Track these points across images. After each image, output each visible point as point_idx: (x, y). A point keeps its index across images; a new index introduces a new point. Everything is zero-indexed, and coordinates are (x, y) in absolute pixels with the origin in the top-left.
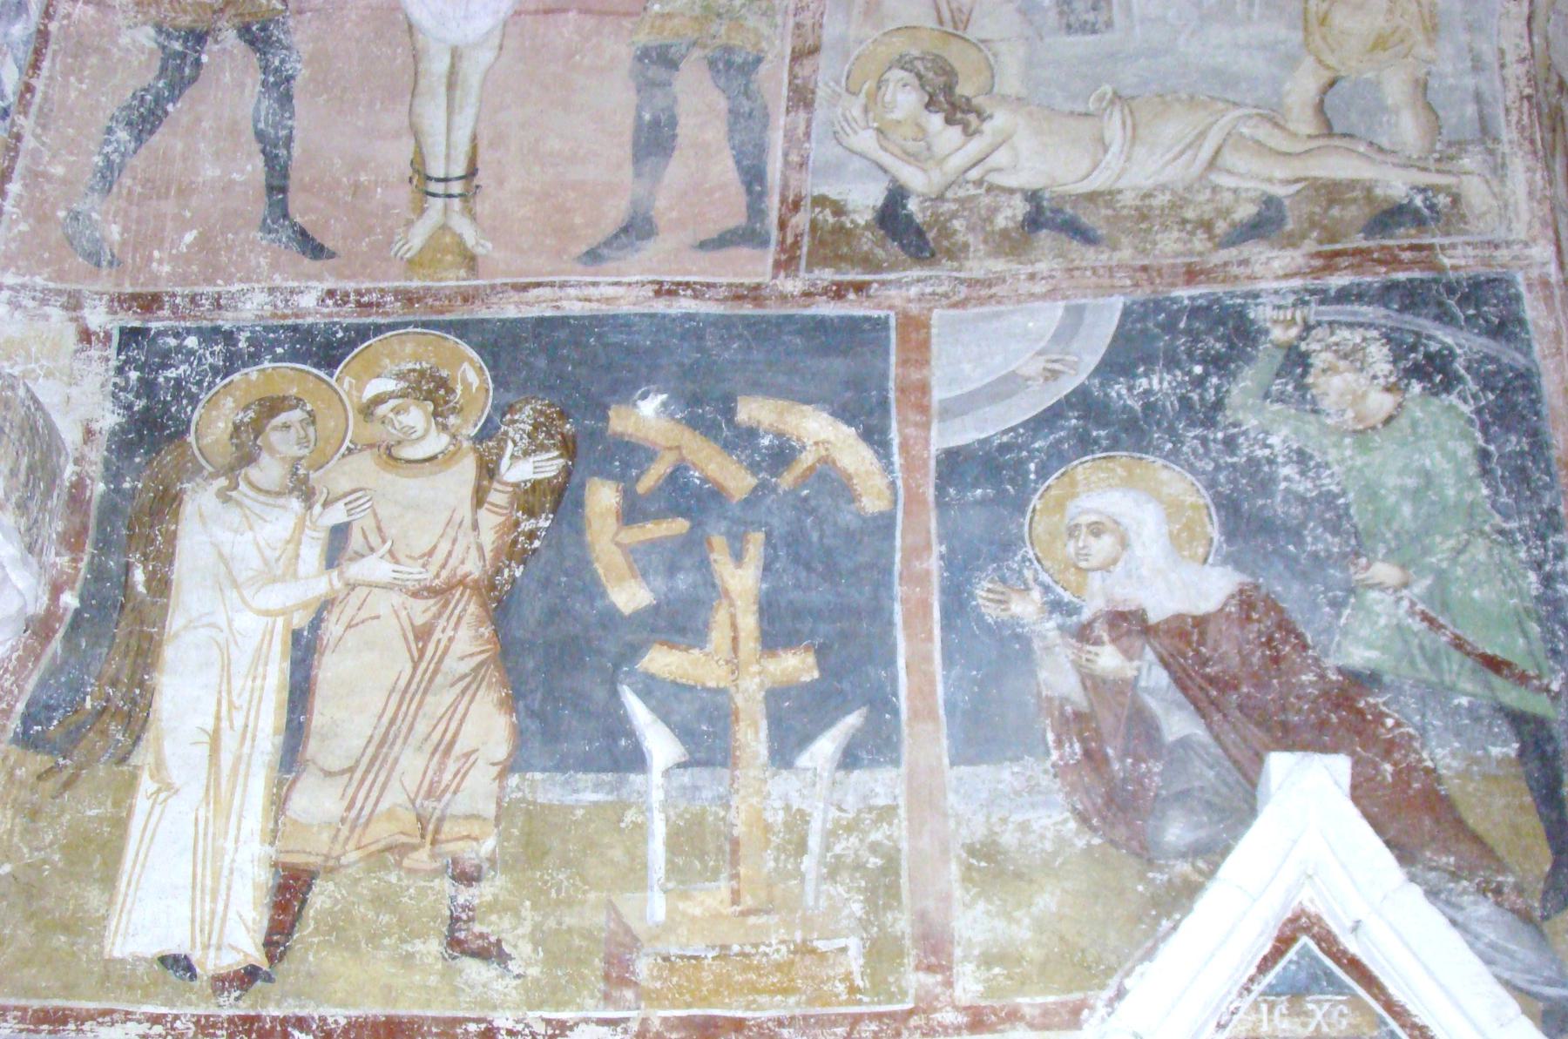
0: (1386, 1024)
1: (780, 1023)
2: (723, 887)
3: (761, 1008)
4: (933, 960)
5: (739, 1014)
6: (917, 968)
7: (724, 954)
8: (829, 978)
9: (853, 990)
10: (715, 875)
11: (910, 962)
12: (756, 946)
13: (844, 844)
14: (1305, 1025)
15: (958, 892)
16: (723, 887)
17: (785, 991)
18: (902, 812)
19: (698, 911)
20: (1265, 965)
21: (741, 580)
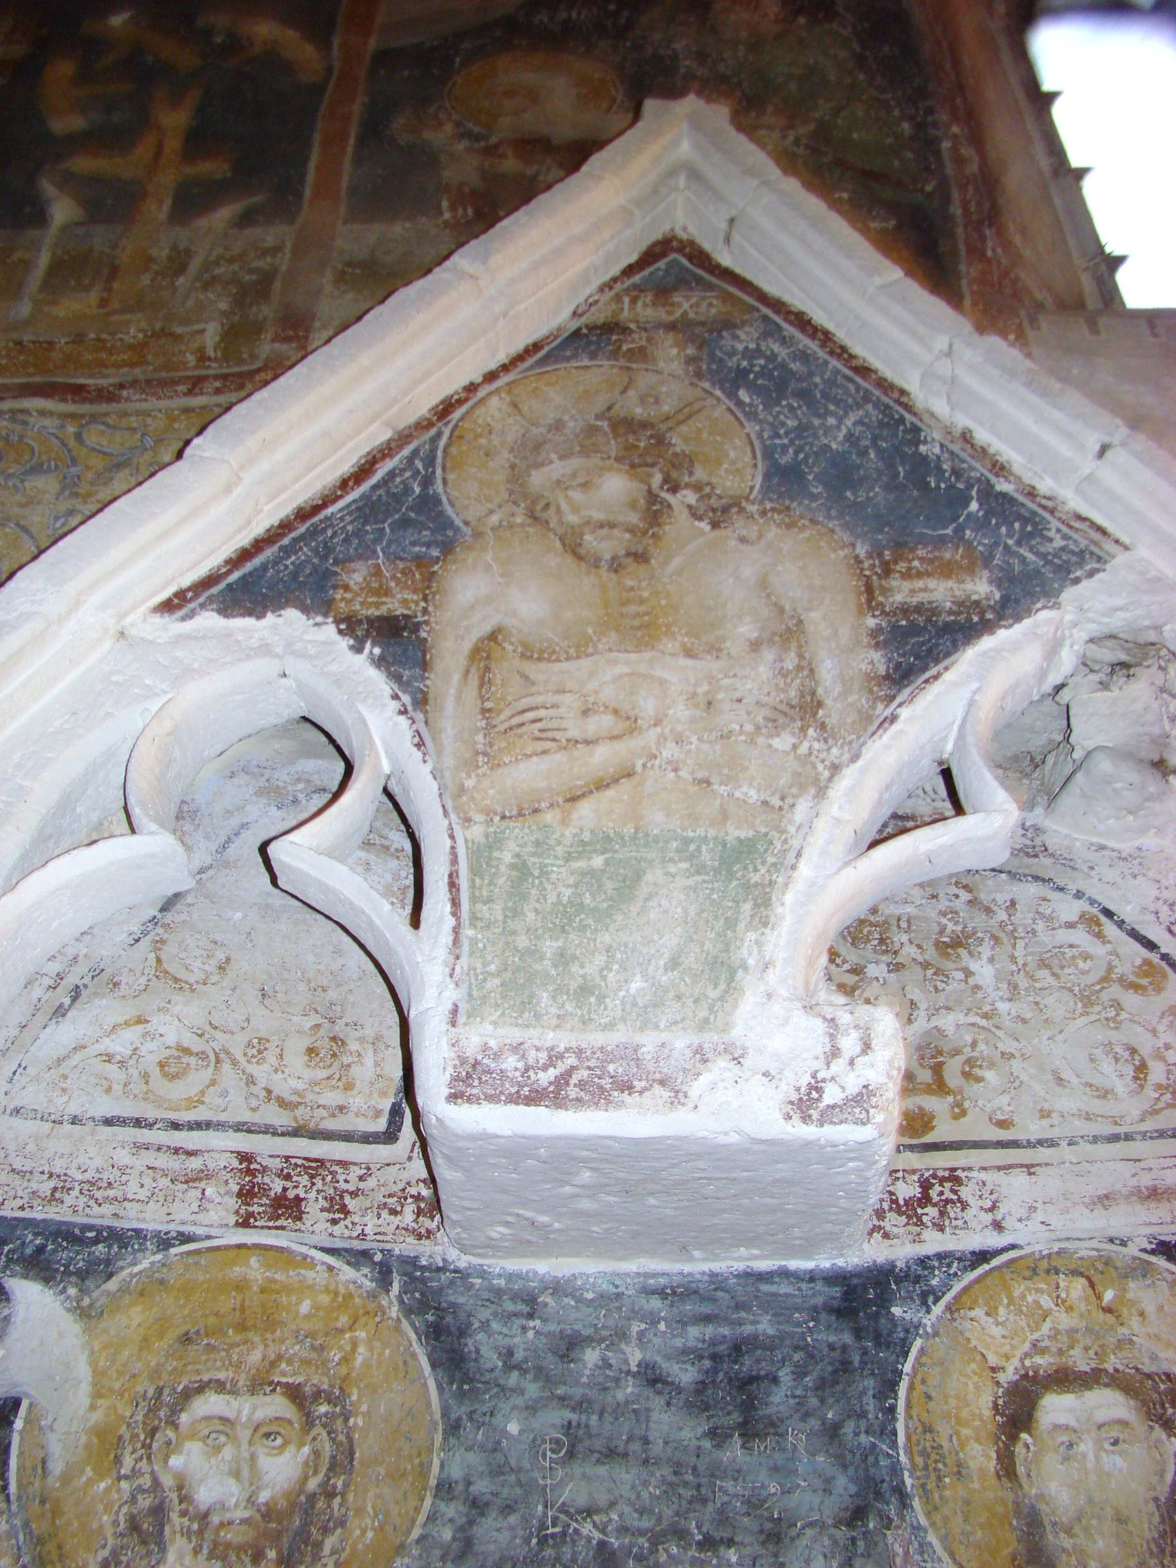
0: (758, 310)
1: (122, 386)
2: (94, 297)
3: (104, 376)
4: (291, 333)
5: (82, 381)
6: (273, 341)
7: (79, 339)
8: (180, 352)
9: (202, 358)
10: (87, 288)
11: (267, 336)
12: (113, 334)
13: (222, 269)
14: (670, 313)
15: (328, 288)
16: (94, 297)
17: (132, 365)
18: (288, 250)
19: (62, 314)
20: (629, 271)
21: (174, 120)
